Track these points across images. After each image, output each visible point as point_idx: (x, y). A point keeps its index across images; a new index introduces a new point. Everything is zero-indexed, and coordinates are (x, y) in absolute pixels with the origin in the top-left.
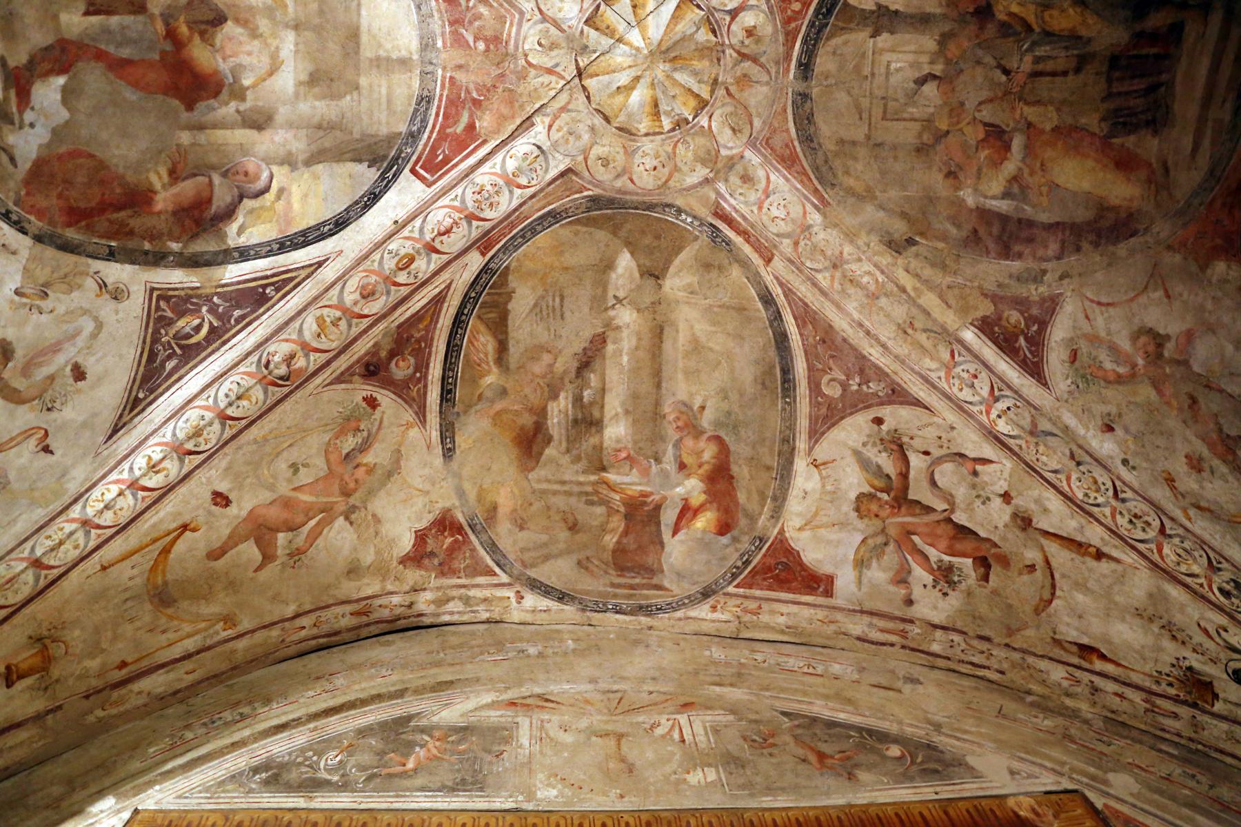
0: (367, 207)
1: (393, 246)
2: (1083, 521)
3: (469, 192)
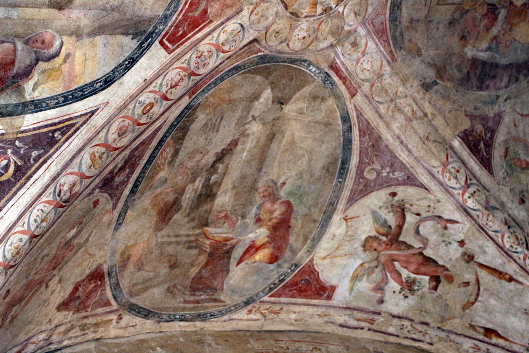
0: (128, 69)
1: (142, 98)
2: (506, 260)
3: (194, 56)
